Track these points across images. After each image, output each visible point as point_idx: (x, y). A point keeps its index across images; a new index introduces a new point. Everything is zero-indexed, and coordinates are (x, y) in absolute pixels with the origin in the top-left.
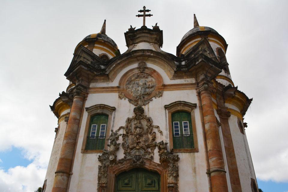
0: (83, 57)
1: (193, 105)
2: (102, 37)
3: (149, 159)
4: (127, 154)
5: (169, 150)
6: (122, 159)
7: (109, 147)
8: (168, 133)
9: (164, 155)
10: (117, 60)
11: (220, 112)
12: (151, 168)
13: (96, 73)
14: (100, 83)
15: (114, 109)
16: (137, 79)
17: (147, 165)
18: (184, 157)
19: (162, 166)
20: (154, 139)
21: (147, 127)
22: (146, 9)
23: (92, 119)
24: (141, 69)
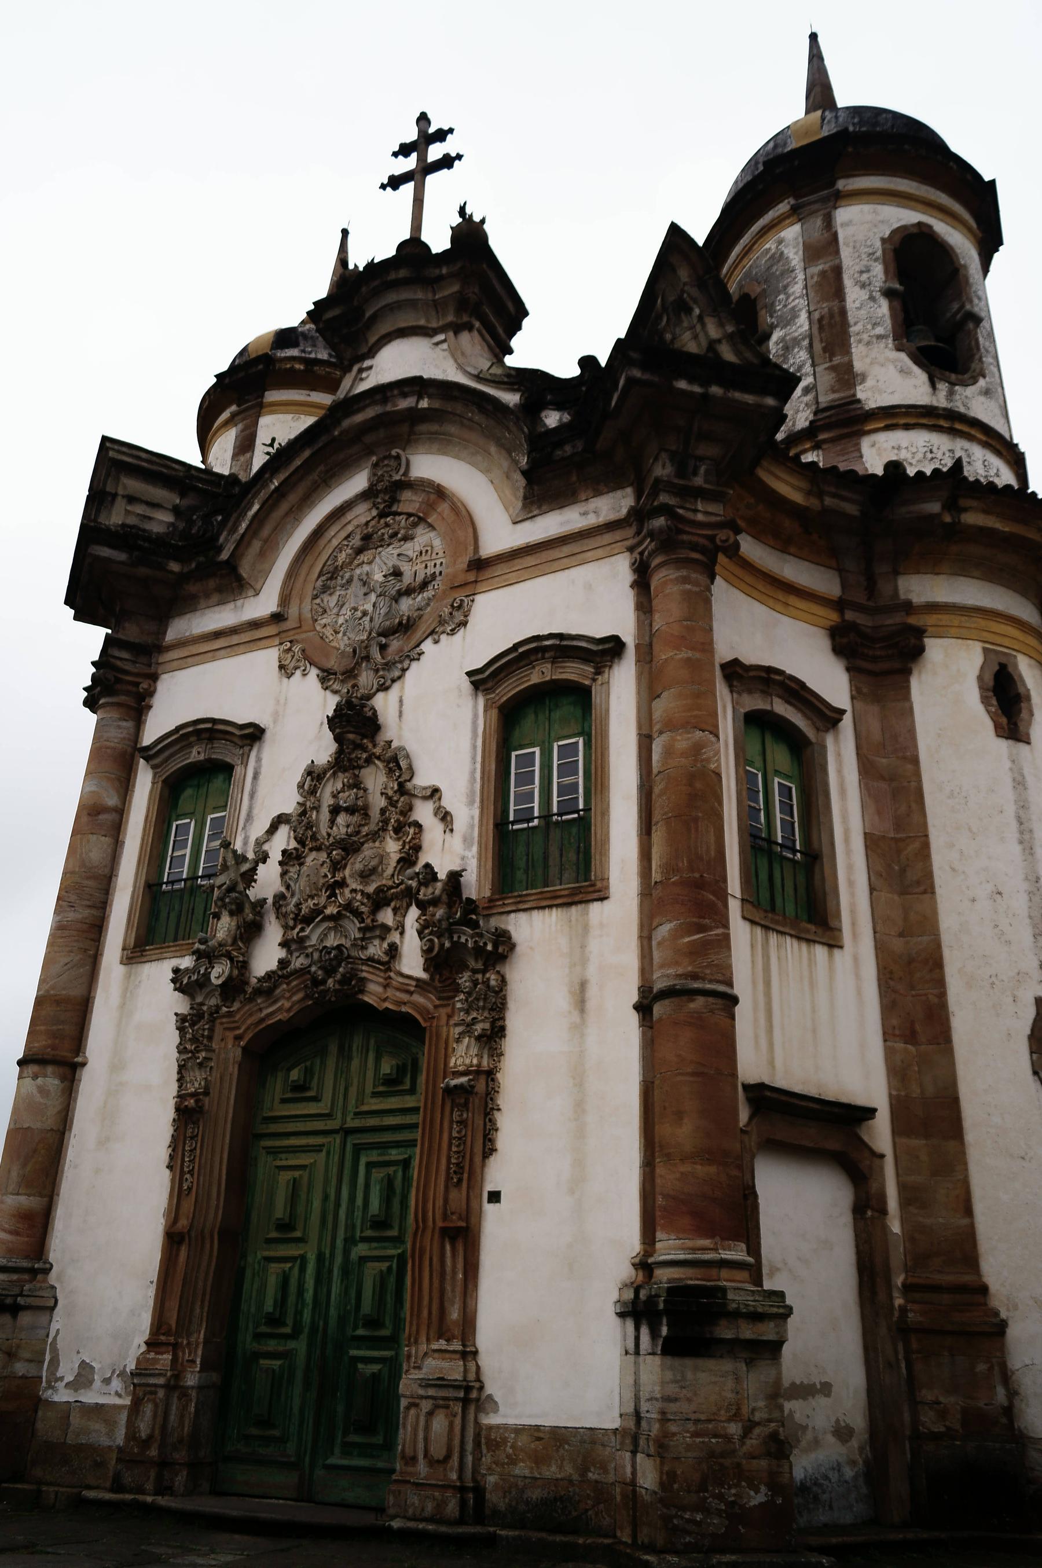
0: (123, 496)
1: (600, 647)
2: (302, 343)
3: (379, 962)
4: (293, 947)
8: (476, 812)
9: (430, 934)
10: (267, 476)
11: (845, 644)
12: (387, 1005)
13: (175, 567)
14: (207, 611)
15: (254, 734)
16: (364, 557)
17: (374, 993)
18: (536, 932)
19: (435, 988)
21: (383, 802)
24: (379, 500)
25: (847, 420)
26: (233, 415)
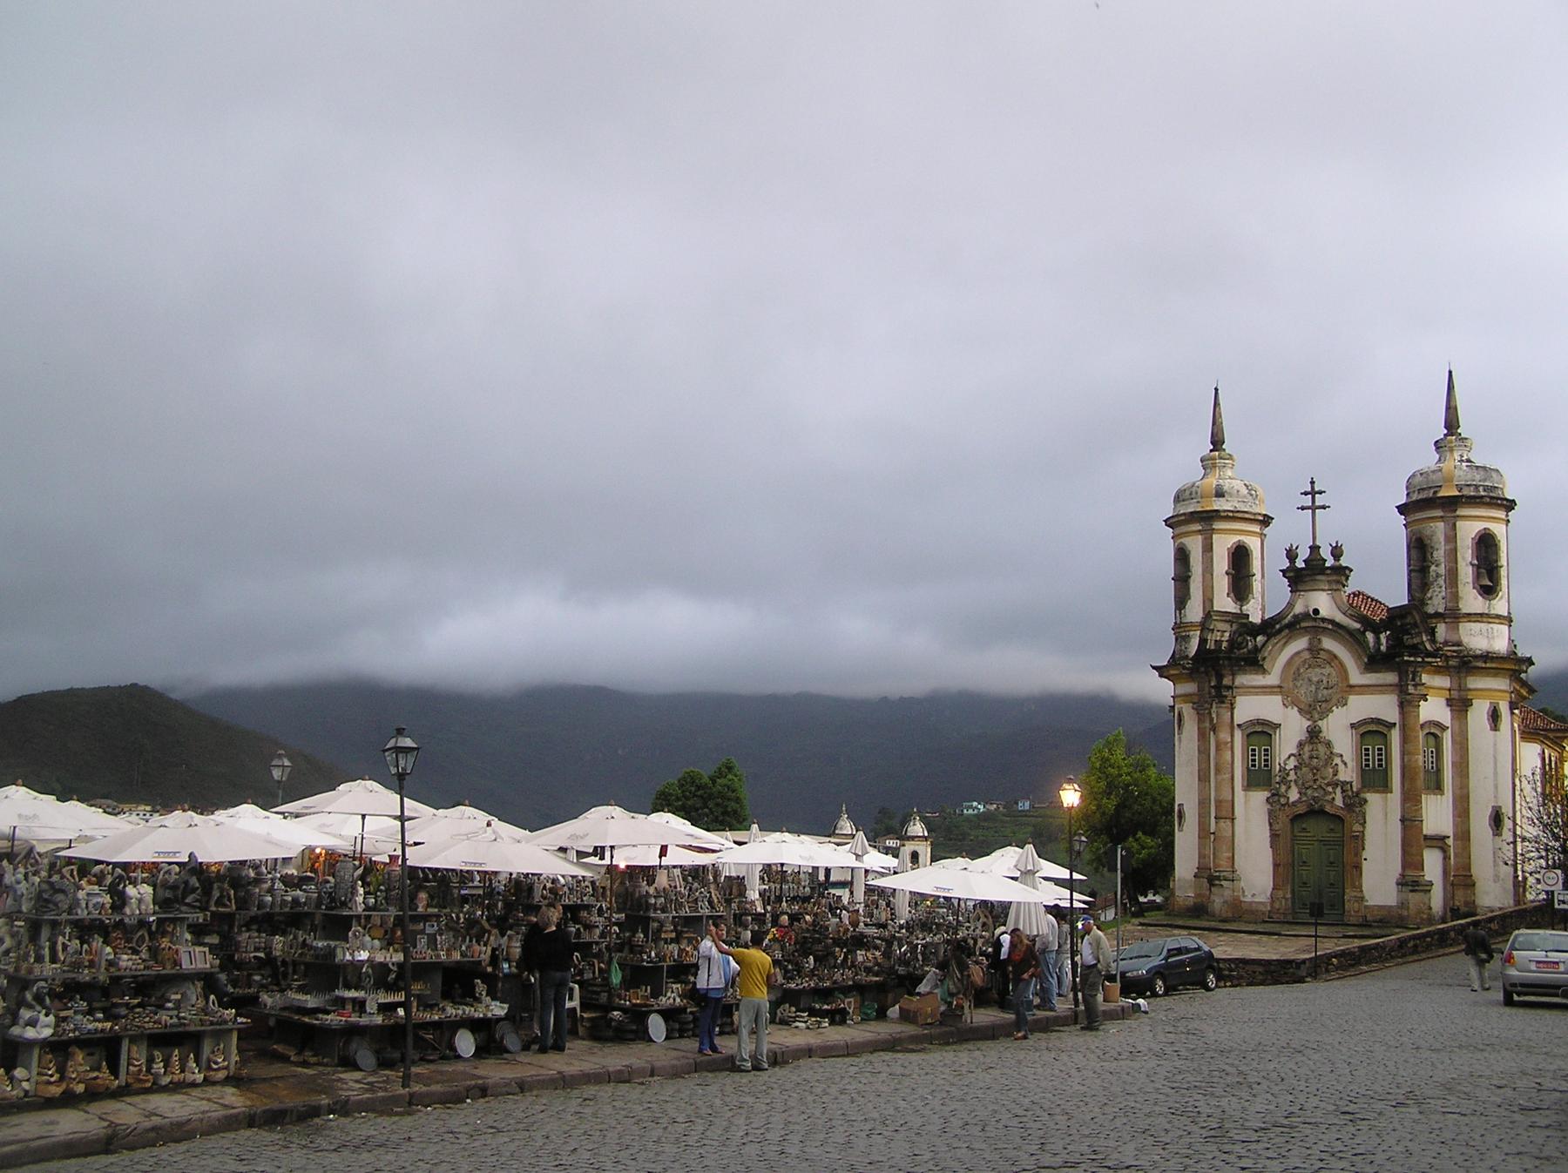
11: (1450, 702)
17: (1328, 808)
18: (1373, 799)
25: (1454, 616)
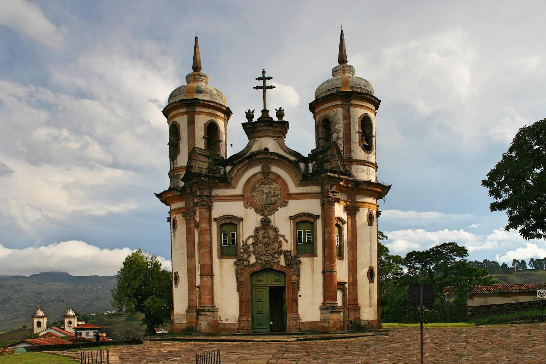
5: (293, 255)
6: (253, 264)
7: (242, 255)
17: (275, 267)
20: (280, 246)
22: (267, 75)
23: (221, 227)
26: (186, 112)
